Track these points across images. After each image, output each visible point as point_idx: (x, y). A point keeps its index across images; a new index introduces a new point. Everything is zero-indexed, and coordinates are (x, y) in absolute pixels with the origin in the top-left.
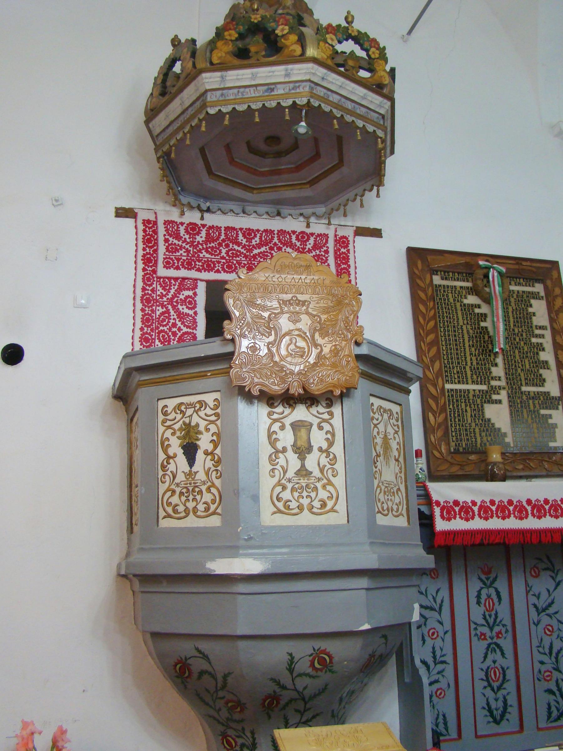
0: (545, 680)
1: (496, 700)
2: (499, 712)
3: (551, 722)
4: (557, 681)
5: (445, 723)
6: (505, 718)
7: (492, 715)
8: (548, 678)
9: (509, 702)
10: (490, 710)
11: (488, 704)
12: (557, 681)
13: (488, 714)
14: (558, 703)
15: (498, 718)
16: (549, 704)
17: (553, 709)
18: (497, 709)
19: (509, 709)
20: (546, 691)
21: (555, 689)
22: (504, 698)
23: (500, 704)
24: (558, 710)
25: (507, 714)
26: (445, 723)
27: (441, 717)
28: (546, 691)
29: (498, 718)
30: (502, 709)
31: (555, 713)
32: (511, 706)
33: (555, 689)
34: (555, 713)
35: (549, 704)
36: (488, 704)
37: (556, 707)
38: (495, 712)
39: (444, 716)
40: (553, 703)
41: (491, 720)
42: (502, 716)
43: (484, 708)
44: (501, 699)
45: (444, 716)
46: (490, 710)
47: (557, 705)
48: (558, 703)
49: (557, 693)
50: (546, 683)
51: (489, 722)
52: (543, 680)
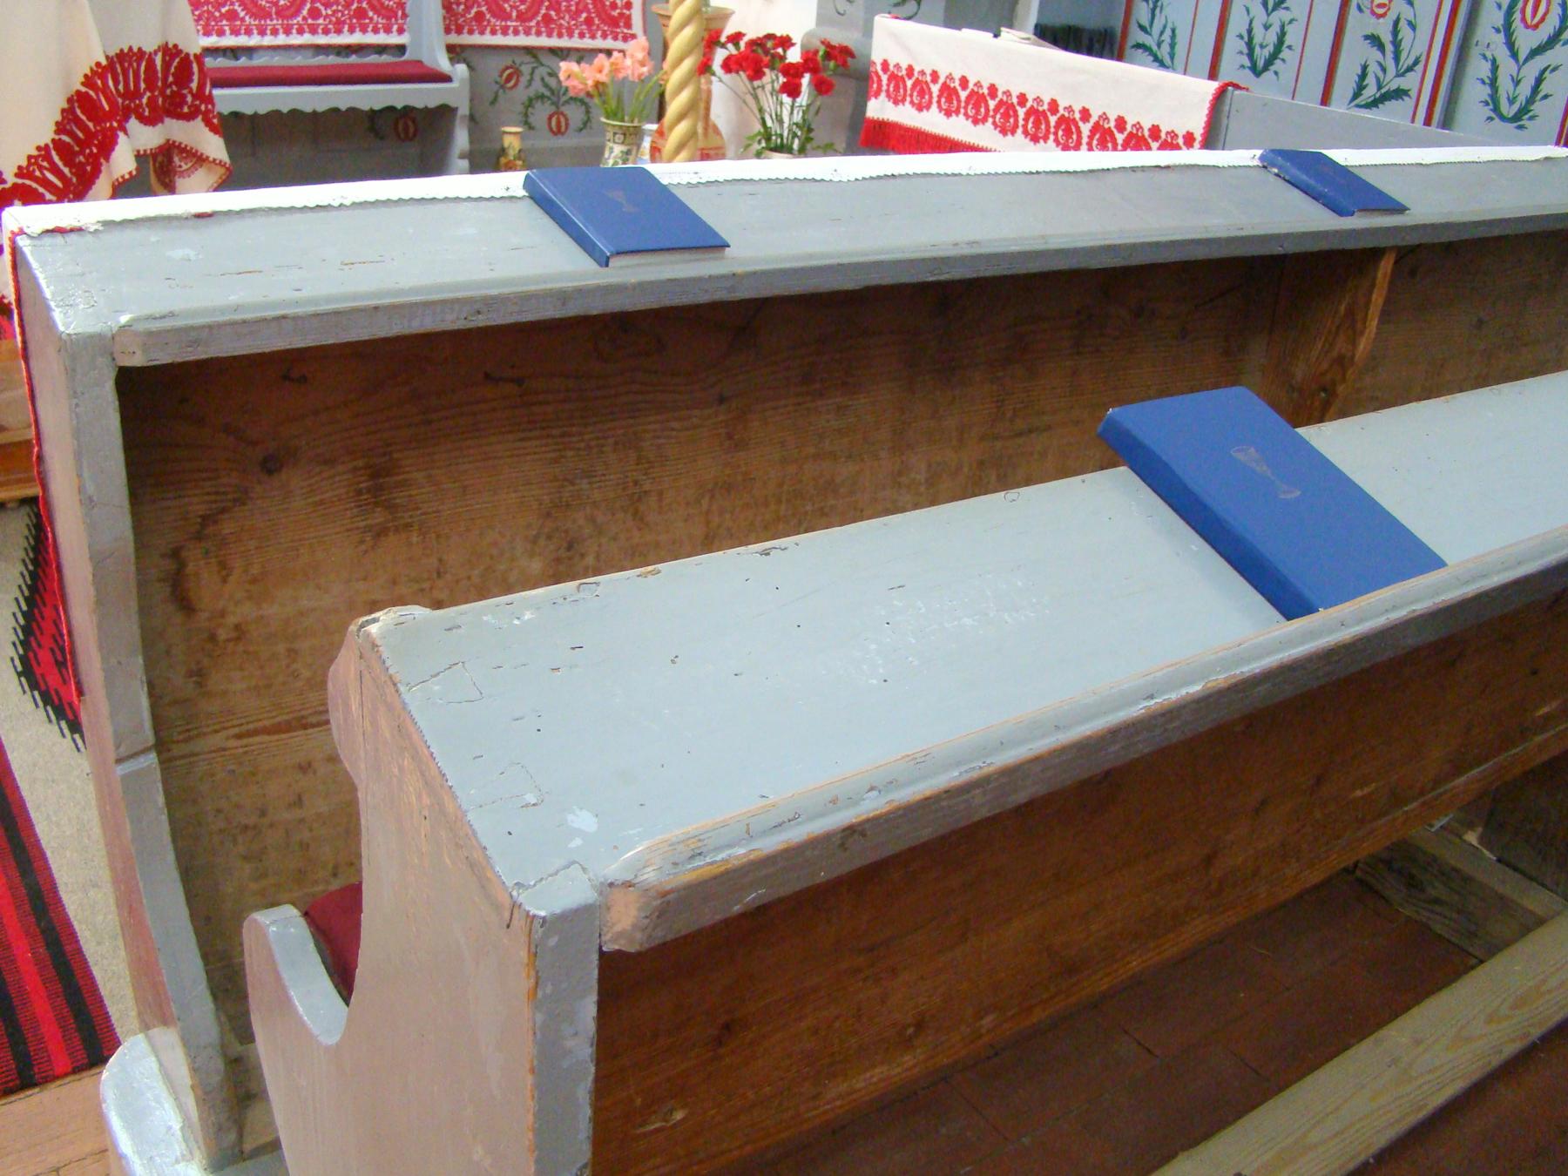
0: (1373, 13)
1: (1267, 27)
2: (1266, 53)
3: (1358, 106)
4: (1396, 23)
5: (1172, 46)
6: (1272, 68)
7: (1251, 55)
8: (1380, 11)
9: (1288, 41)
10: (1250, 45)
11: (1250, 31)
12: (1396, 23)
13: (1245, 51)
14: (1384, 70)
15: (1260, 64)
16: (1365, 68)
17: (1370, 80)
18: (1262, 47)
19: (1285, 54)
20: (1367, 37)
21: (1387, 38)
22: (1282, 27)
23: (1272, 38)
24: (1379, 88)
25: (1278, 62)
26: (1172, 46)
27: (1168, 32)
28: (1367, 37)
29: (1260, 64)
30: (1271, 48)
31: (1370, 92)
32: (1290, 47)
33: (1387, 38)
34: (1370, 92)
35: (1365, 68)
36: (1250, 31)
37: (1378, 79)
38: (1257, 50)
39: (1173, 31)
40: (1373, 69)
41: (1247, 63)
42: (1269, 62)
43: (1241, 37)
44: (1275, 29)
45: (1173, 31)
46: (1250, 45)
47: (1380, 74)
48: (1384, 70)
49: (1389, 48)
50: (1373, 20)
51: (1242, 66)
52: (1367, 12)
